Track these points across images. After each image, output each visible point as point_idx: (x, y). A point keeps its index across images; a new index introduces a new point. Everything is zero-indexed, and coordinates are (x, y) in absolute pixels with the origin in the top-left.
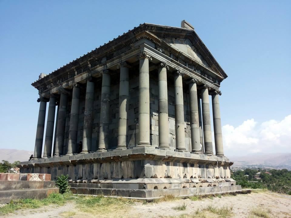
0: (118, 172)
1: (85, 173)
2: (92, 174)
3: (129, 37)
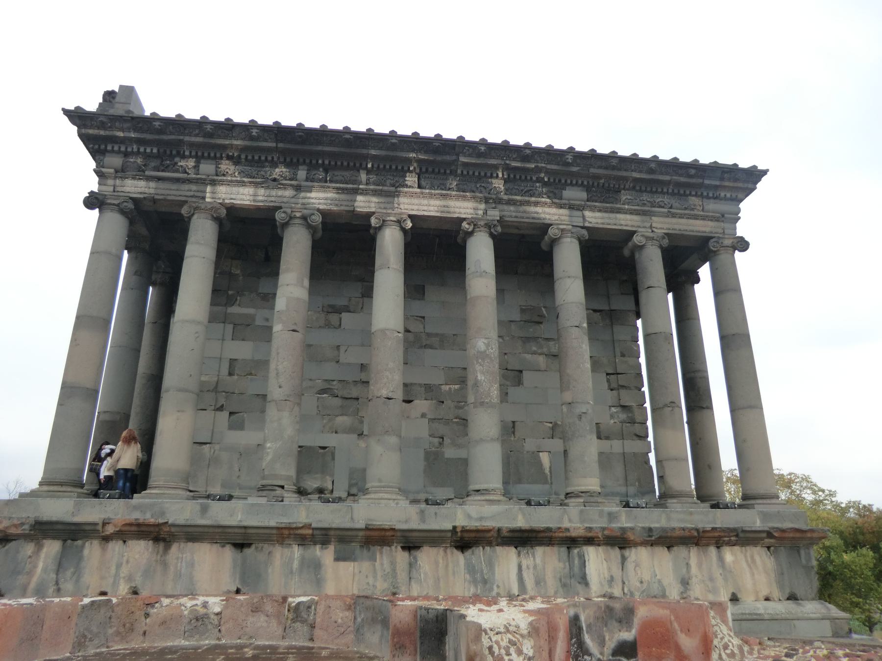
0: (711, 579)
1: (539, 582)
2: (580, 588)
3: (703, 178)
